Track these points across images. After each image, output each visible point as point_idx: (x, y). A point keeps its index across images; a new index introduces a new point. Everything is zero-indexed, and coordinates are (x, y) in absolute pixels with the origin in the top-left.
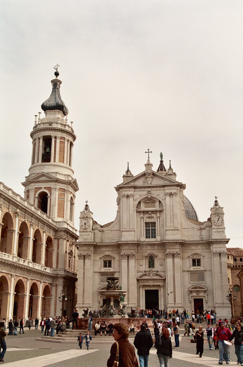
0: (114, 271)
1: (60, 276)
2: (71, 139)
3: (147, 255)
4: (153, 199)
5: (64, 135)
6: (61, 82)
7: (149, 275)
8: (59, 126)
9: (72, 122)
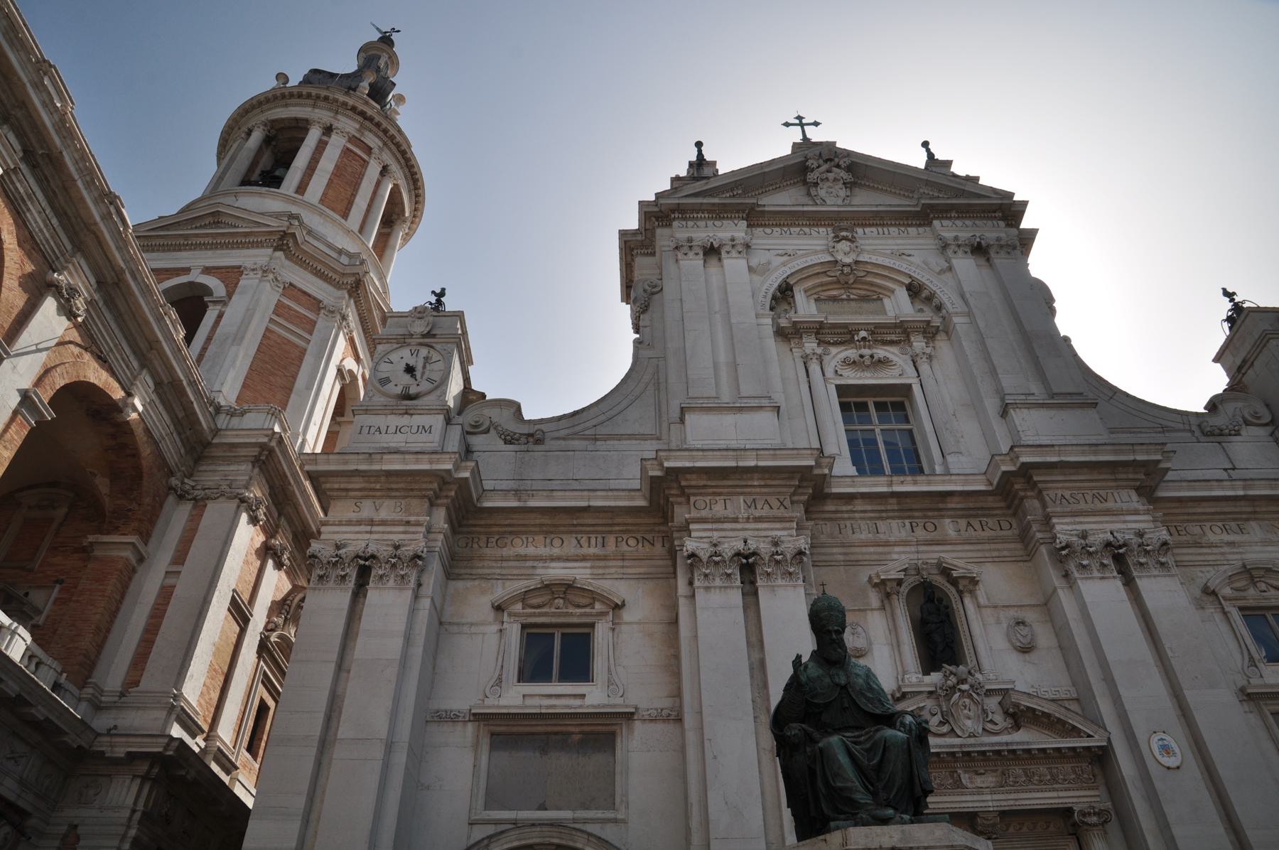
0: (617, 703)
1: (120, 752)
3: (901, 576)
4: (869, 279)
7: (945, 729)
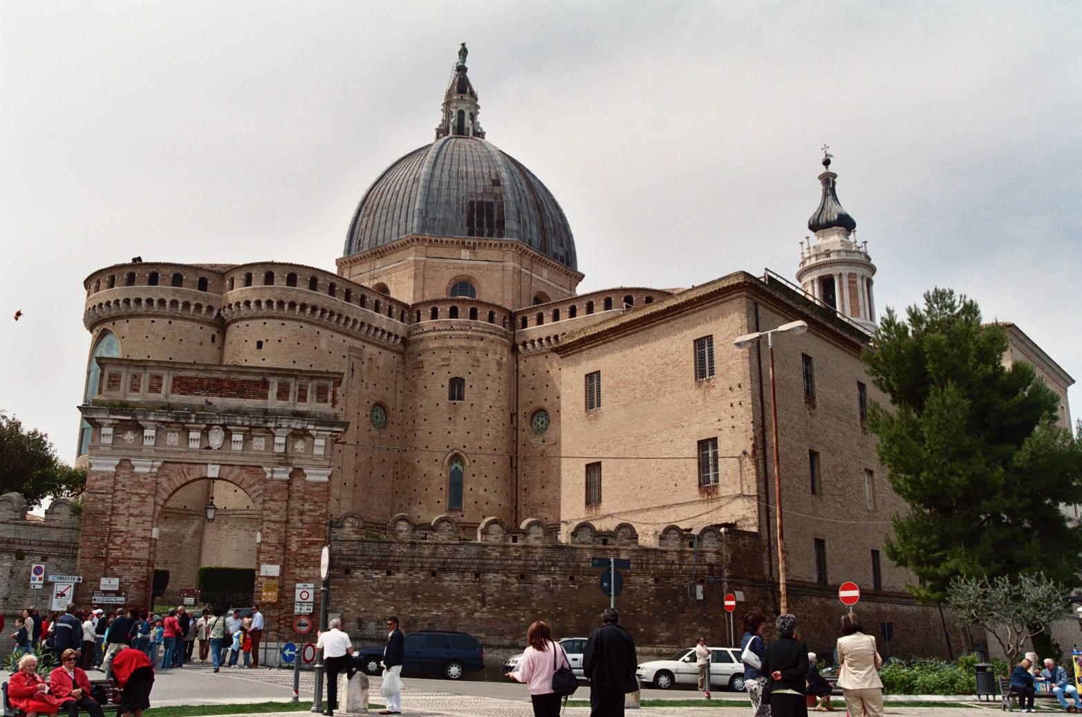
2: (866, 272)
5: (852, 270)
6: (835, 176)
8: (843, 256)
9: (865, 242)
